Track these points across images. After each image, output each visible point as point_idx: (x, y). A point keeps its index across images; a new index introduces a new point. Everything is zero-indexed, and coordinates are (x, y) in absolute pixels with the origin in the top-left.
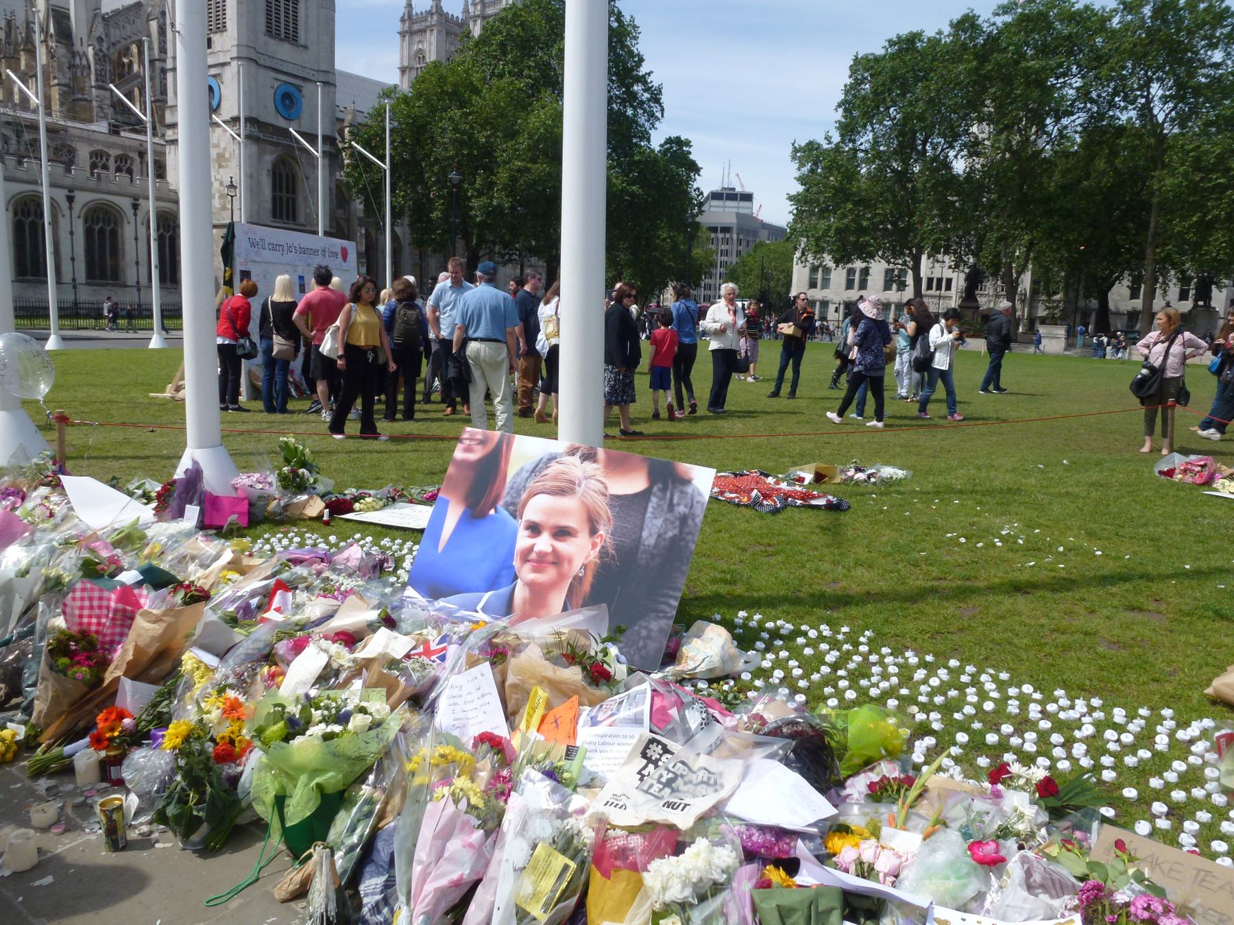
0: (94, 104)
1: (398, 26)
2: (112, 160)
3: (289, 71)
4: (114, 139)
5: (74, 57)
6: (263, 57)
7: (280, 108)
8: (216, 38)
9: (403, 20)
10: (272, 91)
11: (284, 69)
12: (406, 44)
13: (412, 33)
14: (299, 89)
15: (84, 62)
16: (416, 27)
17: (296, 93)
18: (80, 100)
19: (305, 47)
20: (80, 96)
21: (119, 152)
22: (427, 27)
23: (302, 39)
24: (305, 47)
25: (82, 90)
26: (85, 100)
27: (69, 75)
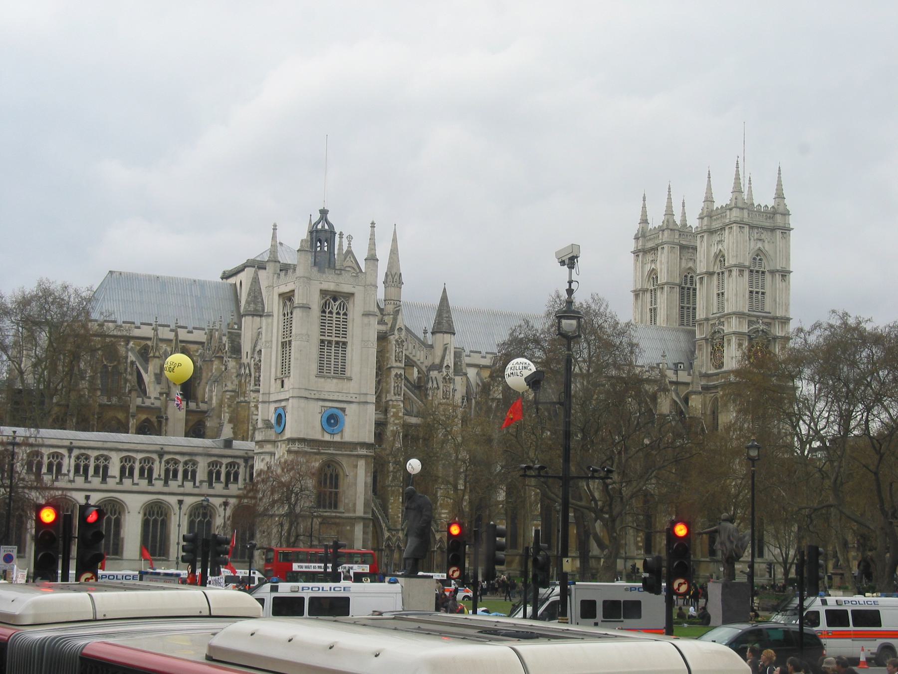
0: (252, 404)
1: (632, 245)
2: (224, 467)
3: (335, 398)
4: (228, 452)
5: (240, 368)
6: (313, 393)
7: (326, 426)
8: (286, 380)
9: (637, 238)
10: (320, 416)
11: (331, 398)
12: (639, 264)
13: (645, 251)
14: (343, 410)
15: (247, 371)
16: (650, 245)
17: (339, 413)
18: (242, 402)
19: (350, 379)
20: (242, 399)
21: (230, 460)
22: (658, 245)
23: (348, 374)
24: (350, 379)
25: (244, 394)
26: (245, 402)
27: (236, 382)
